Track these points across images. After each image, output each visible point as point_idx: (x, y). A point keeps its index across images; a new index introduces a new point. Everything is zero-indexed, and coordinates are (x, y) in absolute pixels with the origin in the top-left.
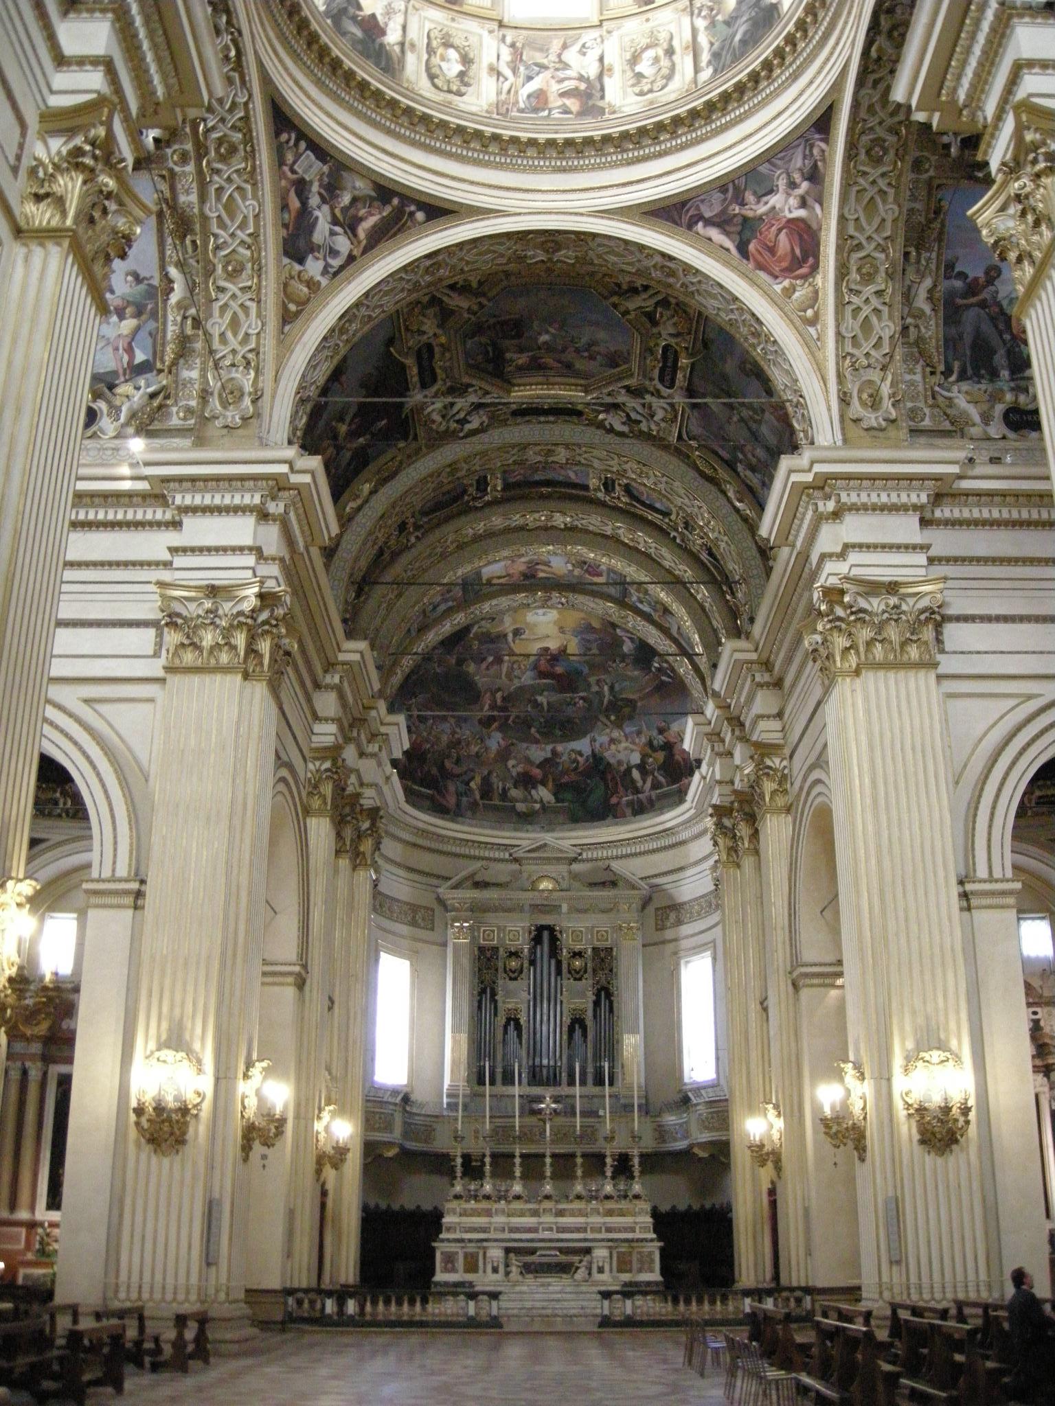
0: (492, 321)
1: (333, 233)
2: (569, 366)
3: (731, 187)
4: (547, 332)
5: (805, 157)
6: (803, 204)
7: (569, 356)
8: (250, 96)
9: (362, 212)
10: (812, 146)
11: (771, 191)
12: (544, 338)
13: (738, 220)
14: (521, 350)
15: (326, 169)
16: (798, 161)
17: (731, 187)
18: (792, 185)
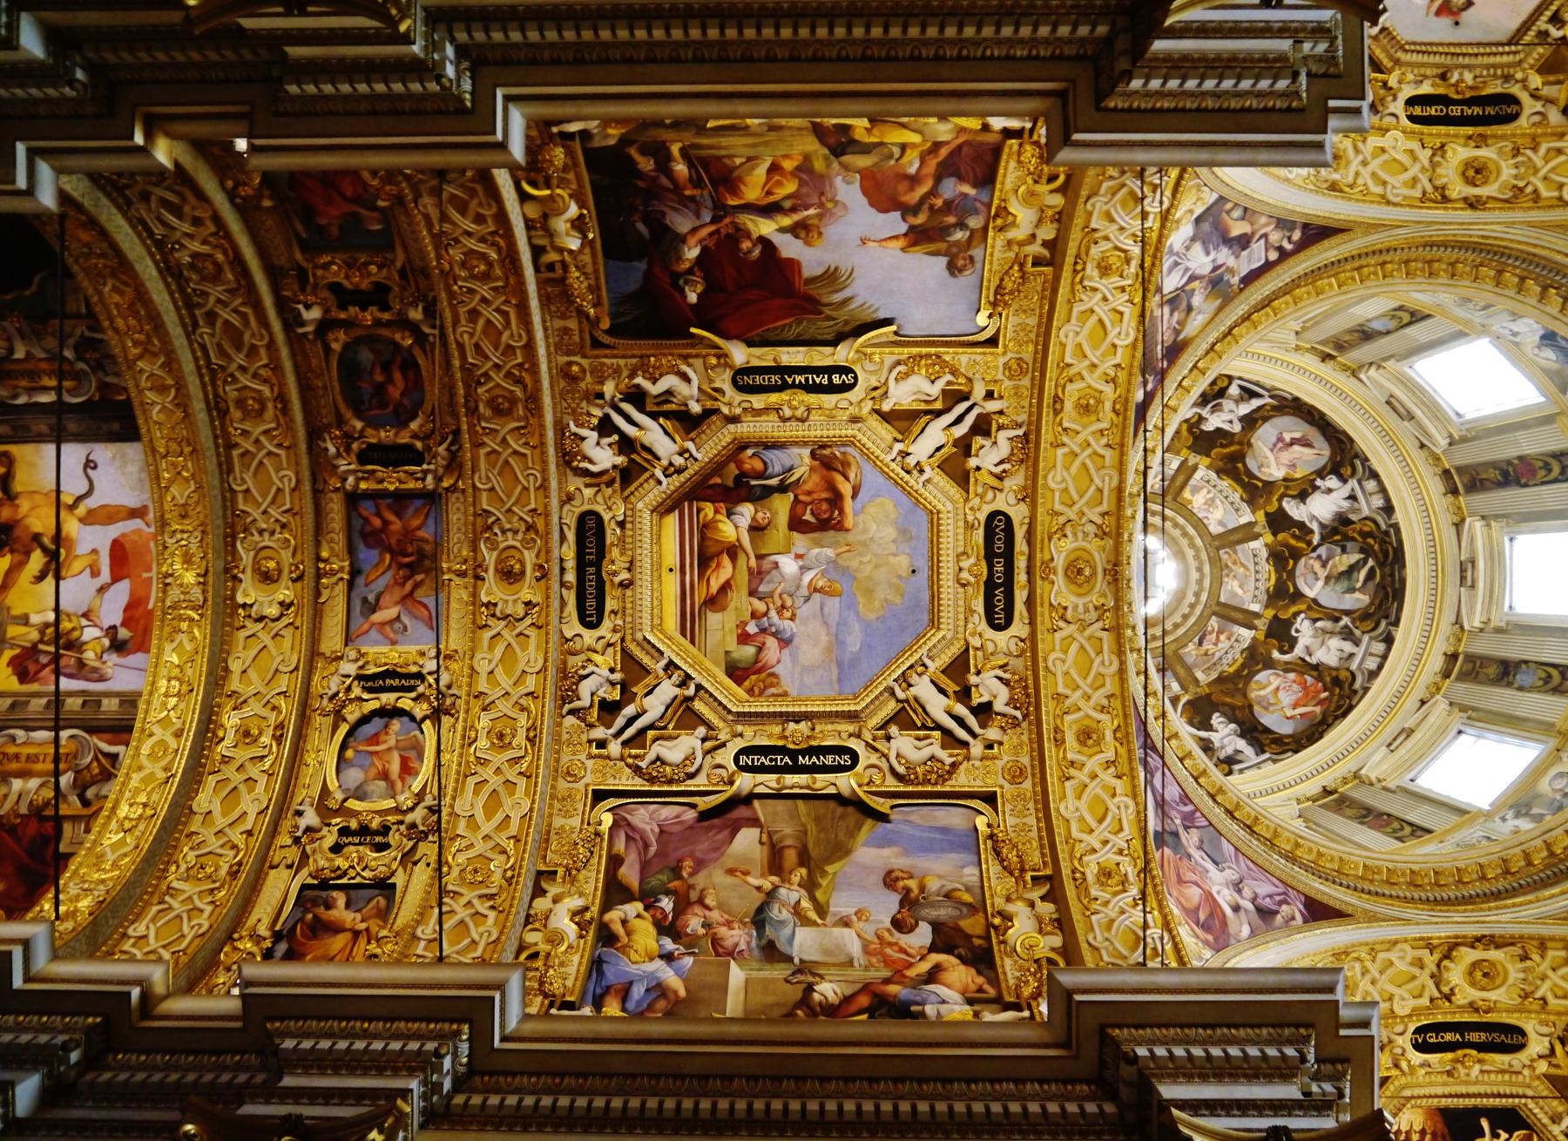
0: (846, 488)
1: (1187, 269)
2: (714, 602)
3: (1190, 808)
4: (804, 569)
5: (1270, 896)
6: (1236, 909)
7: (740, 601)
8: (1395, 204)
9: (1176, 316)
10: (1285, 902)
11: (1216, 863)
12: (788, 565)
13: (1173, 828)
14: (756, 529)
15: (1235, 280)
16: (1264, 889)
17: (1190, 808)
18: (1237, 887)
